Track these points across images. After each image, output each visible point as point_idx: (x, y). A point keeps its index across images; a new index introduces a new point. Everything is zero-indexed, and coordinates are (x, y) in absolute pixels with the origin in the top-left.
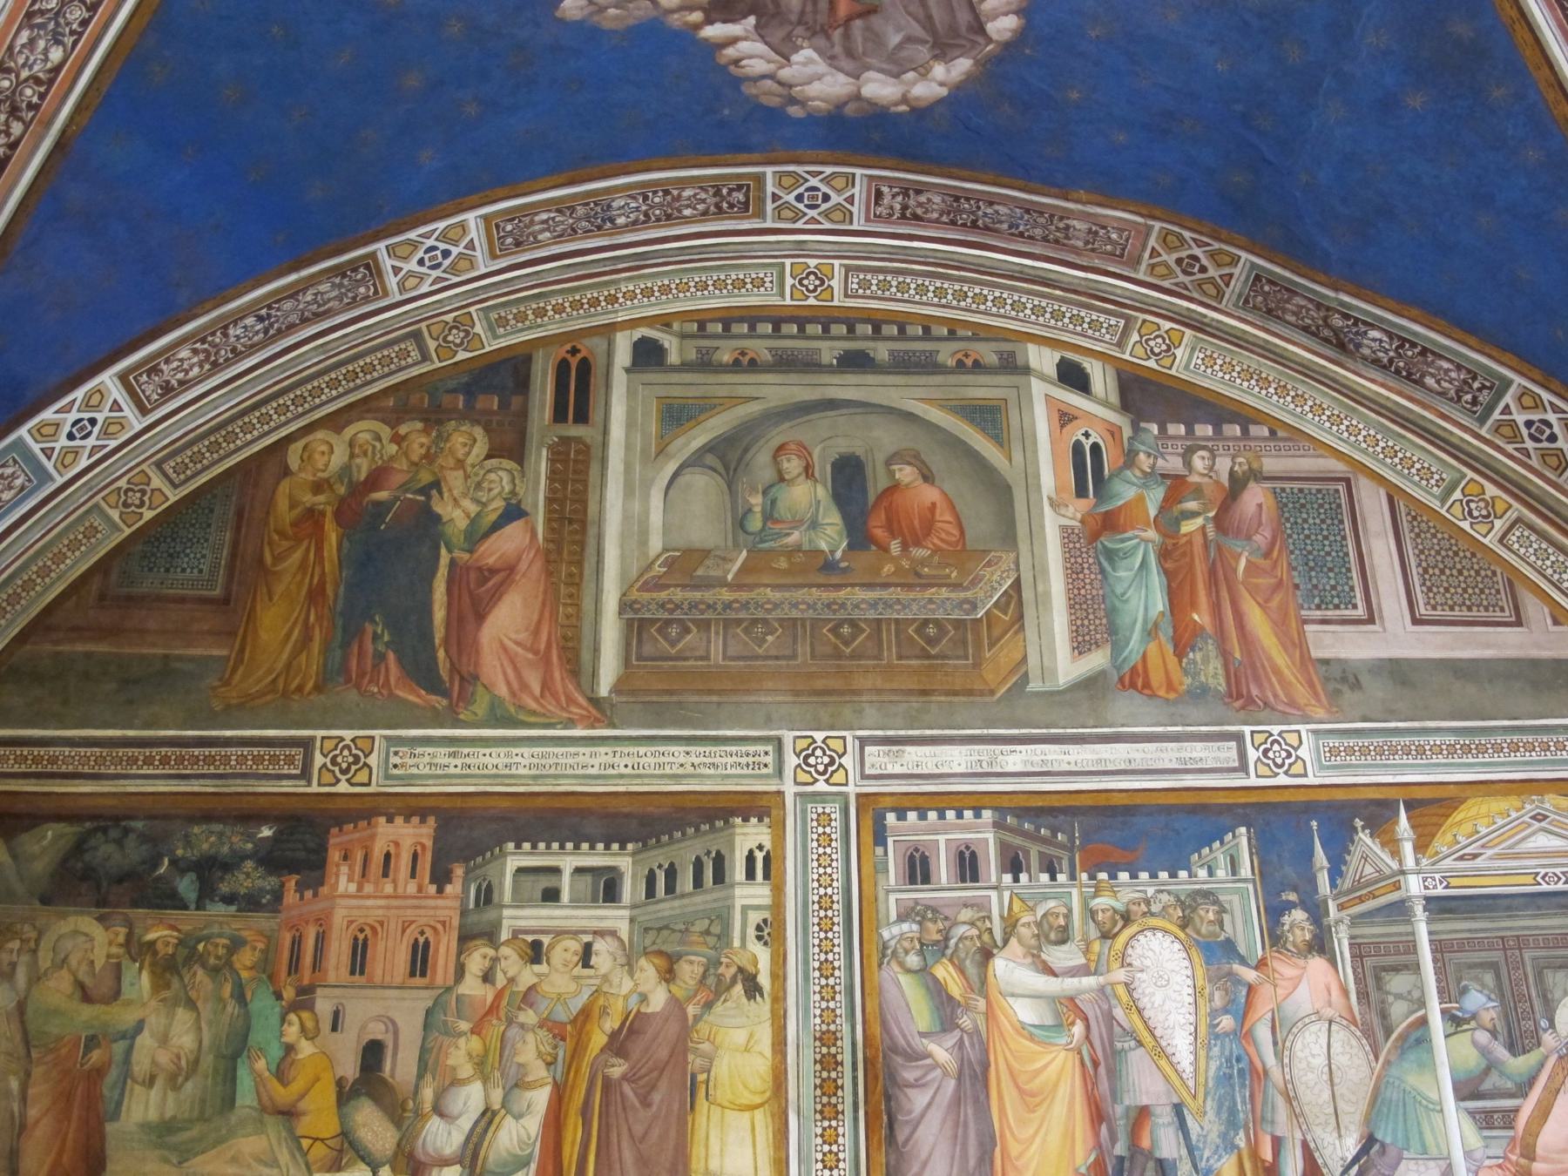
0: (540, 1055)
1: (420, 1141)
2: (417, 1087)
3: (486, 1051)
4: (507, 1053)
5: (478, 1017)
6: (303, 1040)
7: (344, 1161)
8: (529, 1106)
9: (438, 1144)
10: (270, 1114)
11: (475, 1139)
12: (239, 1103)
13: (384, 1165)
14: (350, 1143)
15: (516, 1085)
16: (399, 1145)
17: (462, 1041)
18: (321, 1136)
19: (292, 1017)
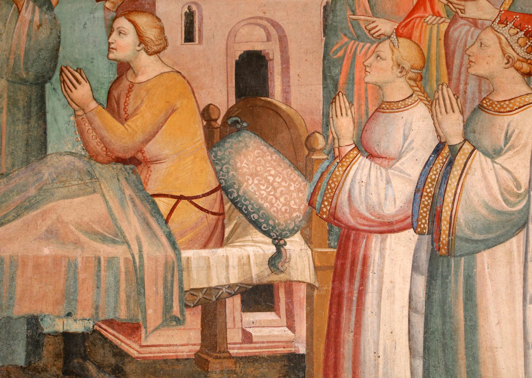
0: (509, 62)
1: (344, 196)
2: (326, 116)
3: (425, 60)
4: (457, 62)
5: (404, 15)
6: (143, 55)
7: (228, 231)
8: (507, 138)
9: (374, 199)
10: (101, 163)
11: (429, 189)
12: (49, 151)
13: (293, 232)
14: (234, 202)
15: (481, 107)
16: (311, 203)
17: (385, 48)
18: (186, 194)
19: (123, 23)
